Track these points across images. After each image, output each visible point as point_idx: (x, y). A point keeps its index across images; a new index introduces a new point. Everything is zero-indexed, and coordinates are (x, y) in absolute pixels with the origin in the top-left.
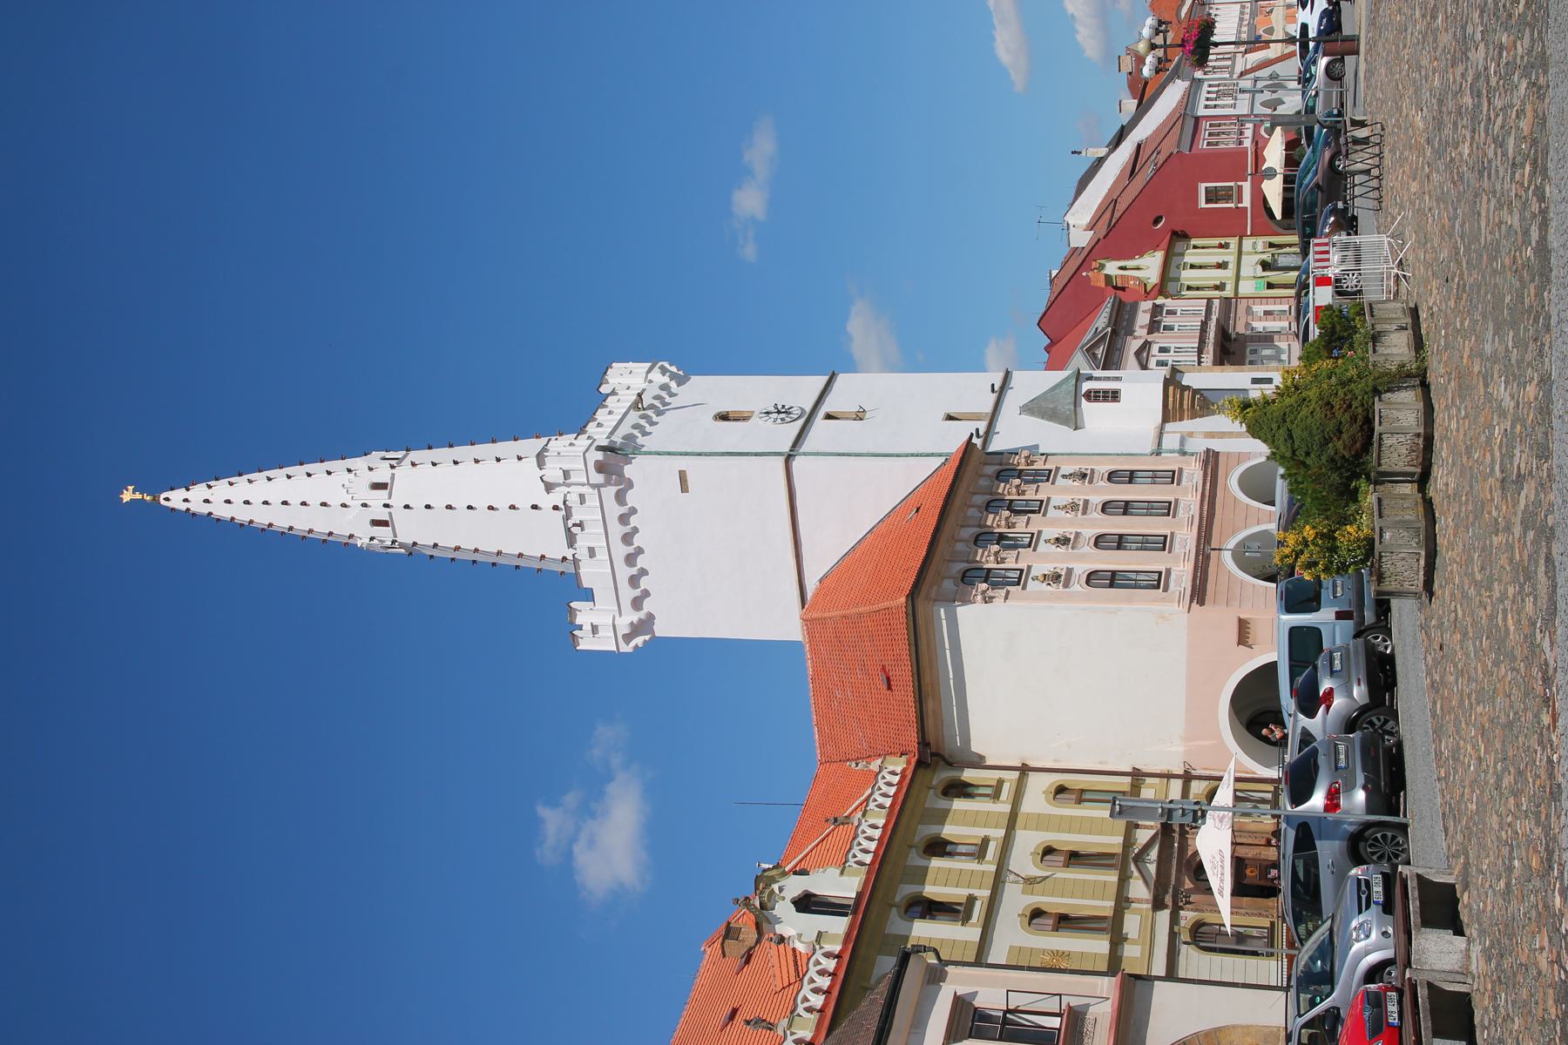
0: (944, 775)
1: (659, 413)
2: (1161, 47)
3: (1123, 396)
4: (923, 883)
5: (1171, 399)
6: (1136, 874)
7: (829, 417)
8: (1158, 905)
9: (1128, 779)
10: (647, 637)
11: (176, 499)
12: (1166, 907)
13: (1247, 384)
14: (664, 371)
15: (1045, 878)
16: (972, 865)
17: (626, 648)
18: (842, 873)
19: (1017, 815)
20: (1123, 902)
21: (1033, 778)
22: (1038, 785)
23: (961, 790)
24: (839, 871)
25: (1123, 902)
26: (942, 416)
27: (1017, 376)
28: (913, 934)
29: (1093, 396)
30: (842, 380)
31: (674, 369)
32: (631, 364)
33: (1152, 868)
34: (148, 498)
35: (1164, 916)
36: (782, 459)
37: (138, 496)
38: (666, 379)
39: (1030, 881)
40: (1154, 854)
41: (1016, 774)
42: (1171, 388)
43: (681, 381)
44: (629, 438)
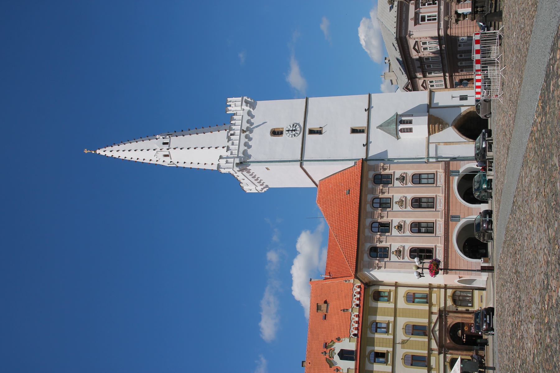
0: (373, 289)
1: (251, 132)
2: (421, 268)
3: (413, 130)
4: (373, 345)
5: (431, 130)
6: (433, 337)
7: (312, 132)
8: (440, 353)
9: (428, 289)
10: (267, 188)
11: (101, 152)
12: (442, 353)
13: (457, 102)
14: (247, 102)
15: (408, 340)
16: (385, 336)
17: (263, 191)
18: (350, 342)
19: (396, 308)
20: (430, 350)
21: (399, 288)
22: (402, 292)
23: (378, 296)
24: (349, 340)
25: (430, 350)
26: (349, 130)
27: (373, 96)
28: (374, 370)
29: (403, 131)
30: (311, 100)
31: (249, 100)
32: (234, 98)
33: (437, 333)
34: (93, 152)
35: (442, 356)
36: (299, 163)
37: (89, 151)
38: (247, 108)
39: (403, 342)
40: (437, 328)
41: (393, 288)
42: (431, 125)
43: (253, 106)
44: (245, 152)
